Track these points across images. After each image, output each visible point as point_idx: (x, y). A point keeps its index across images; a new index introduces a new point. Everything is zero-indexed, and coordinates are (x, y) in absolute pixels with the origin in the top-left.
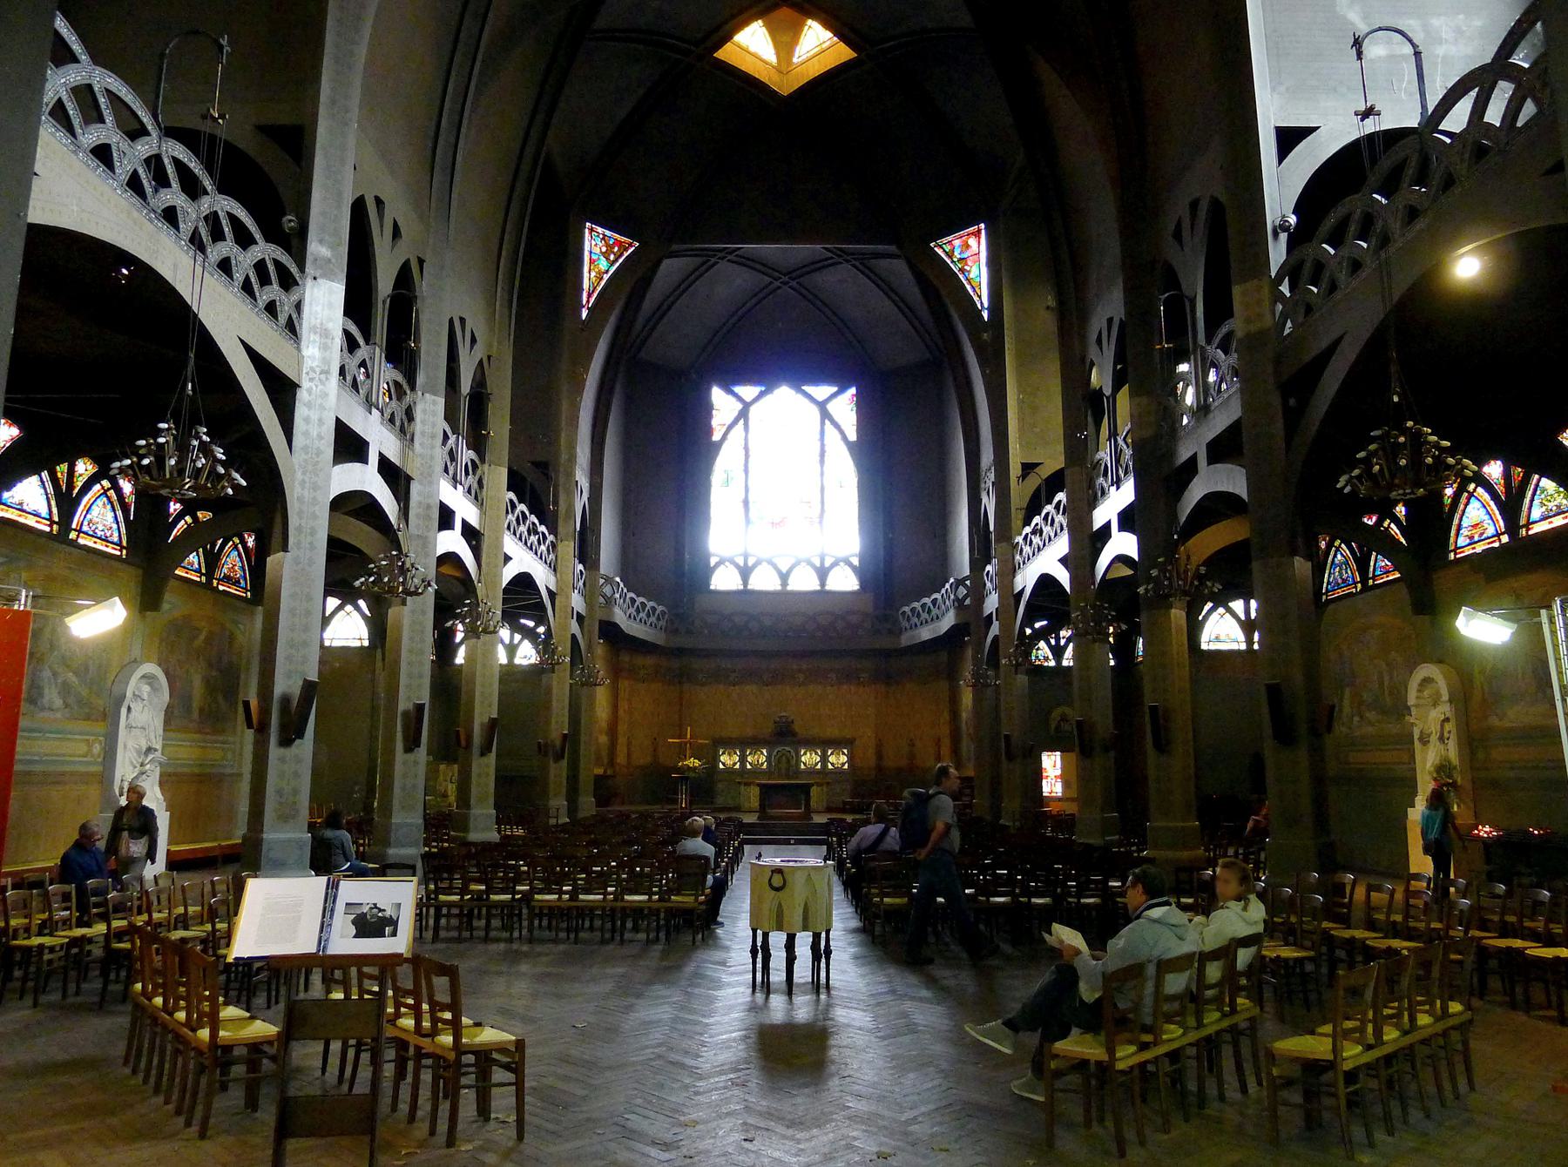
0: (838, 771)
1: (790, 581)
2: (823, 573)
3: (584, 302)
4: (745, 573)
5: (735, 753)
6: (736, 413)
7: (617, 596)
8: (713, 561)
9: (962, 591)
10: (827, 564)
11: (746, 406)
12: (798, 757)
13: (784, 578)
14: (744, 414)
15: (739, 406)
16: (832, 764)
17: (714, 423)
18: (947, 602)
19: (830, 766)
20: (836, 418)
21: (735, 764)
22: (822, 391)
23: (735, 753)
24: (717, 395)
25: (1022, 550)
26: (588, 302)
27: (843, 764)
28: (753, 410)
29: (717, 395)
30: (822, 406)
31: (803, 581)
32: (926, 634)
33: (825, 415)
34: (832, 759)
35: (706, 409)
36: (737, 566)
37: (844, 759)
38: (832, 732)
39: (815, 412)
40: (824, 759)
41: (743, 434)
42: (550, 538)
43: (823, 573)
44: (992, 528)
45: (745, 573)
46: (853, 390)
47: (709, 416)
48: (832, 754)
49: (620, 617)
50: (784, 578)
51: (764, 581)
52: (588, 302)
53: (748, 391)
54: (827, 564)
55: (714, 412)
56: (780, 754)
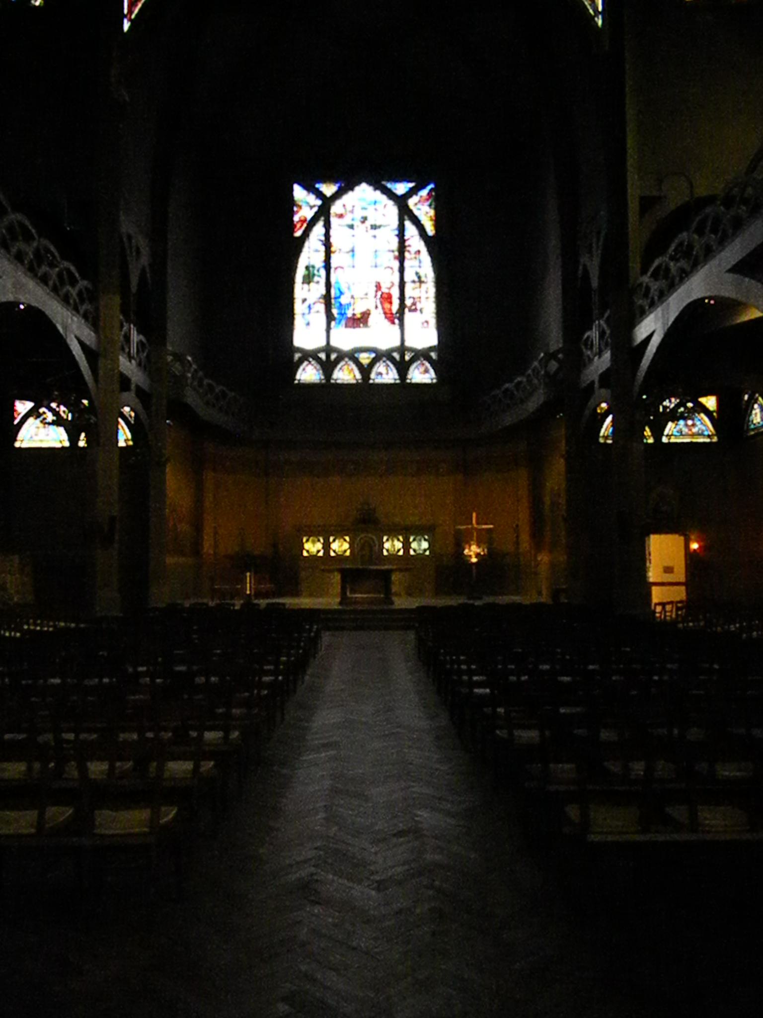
0: (420, 557)
1: (373, 376)
2: (403, 368)
3: (126, 11)
4: (328, 367)
5: (319, 541)
6: (316, 209)
7: (189, 375)
8: (297, 356)
9: (553, 366)
10: (407, 358)
11: (326, 204)
12: (382, 544)
13: (365, 371)
14: (323, 212)
15: (319, 202)
16: (415, 551)
17: (296, 218)
18: (536, 381)
19: (412, 553)
20: (416, 212)
21: (318, 551)
22: (401, 188)
23: (319, 541)
24: (299, 192)
25: (648, 289)
26: (130, 12)
27: (425, 550)
28: (336, 208)
29: (299, 192)
30: (401, 202)
31: (386, 375)
32: (508, 419)
33: (405, 213)
34: (414, 545)
35: (290, 204)
36: (319, 360)
37: (425, 545)
38: (413, 519)
39: (392, 211)
40: (407, 546)
41: (323, 231)
42: (83, 284)
43: (403, 368)
44: (595, 283)
45: (328, 367)
46: (431, 186)
47: (292, 214)
48: (414, 540)
49: (191, 398)
50: (365, 371)
51: (345, 374)
52: (130, 12)
53: (329, 189)
54: (407, 358)
55: (295, 209)
56: (362, 541)
